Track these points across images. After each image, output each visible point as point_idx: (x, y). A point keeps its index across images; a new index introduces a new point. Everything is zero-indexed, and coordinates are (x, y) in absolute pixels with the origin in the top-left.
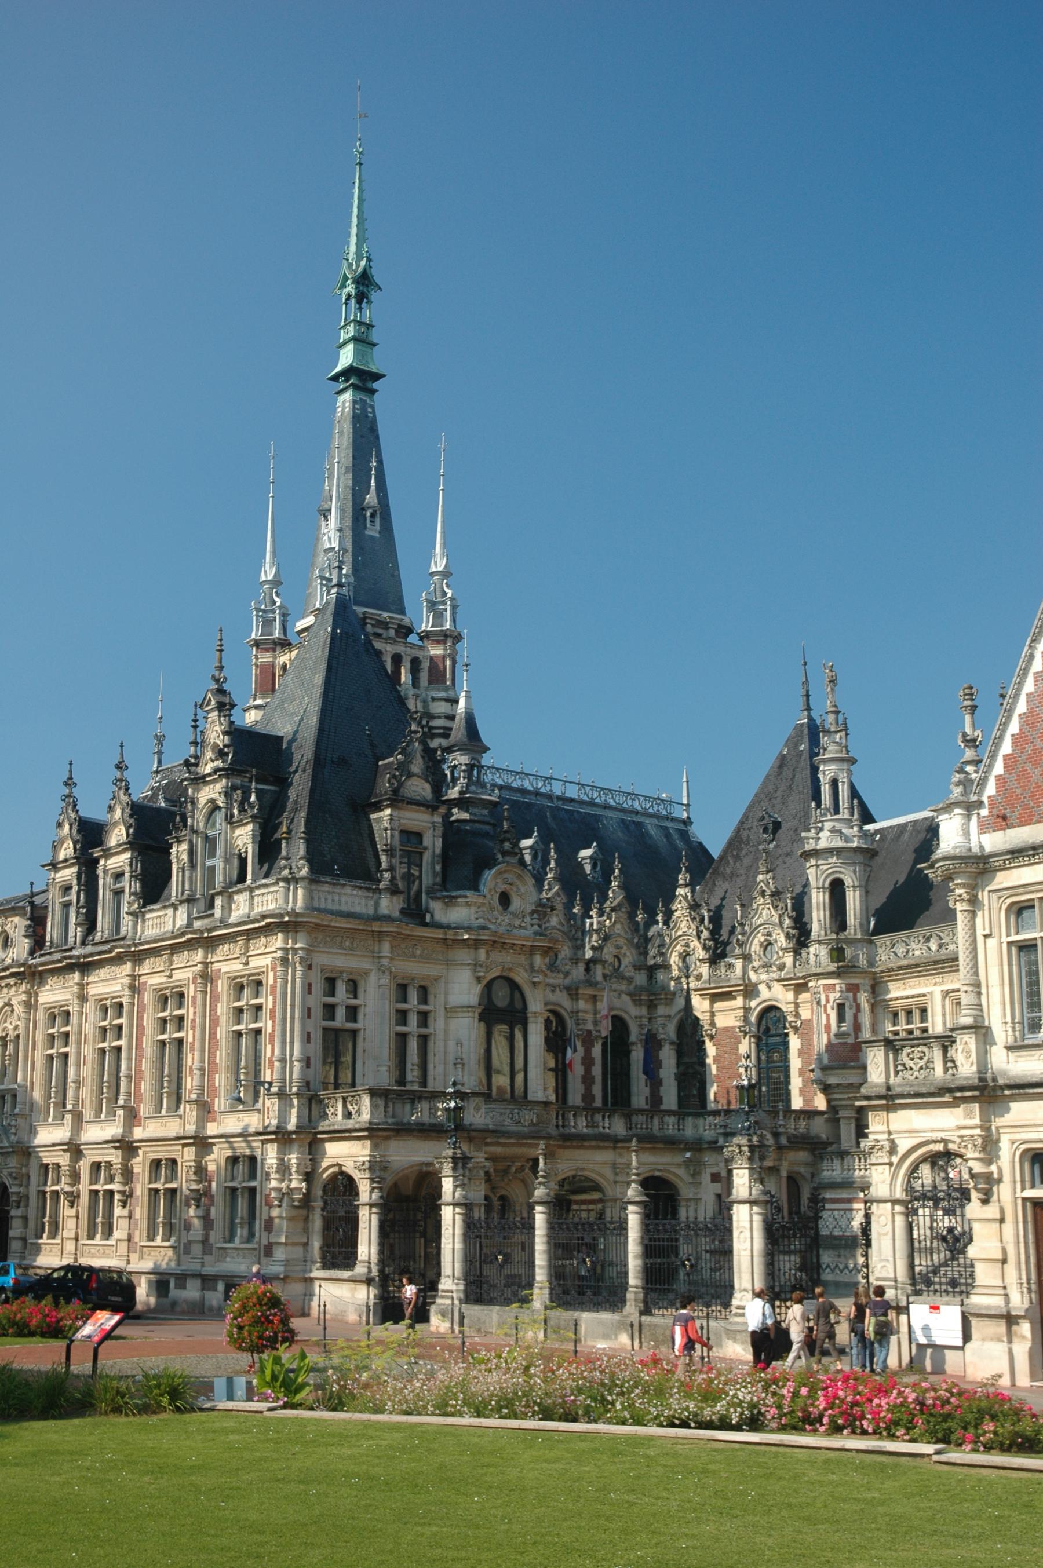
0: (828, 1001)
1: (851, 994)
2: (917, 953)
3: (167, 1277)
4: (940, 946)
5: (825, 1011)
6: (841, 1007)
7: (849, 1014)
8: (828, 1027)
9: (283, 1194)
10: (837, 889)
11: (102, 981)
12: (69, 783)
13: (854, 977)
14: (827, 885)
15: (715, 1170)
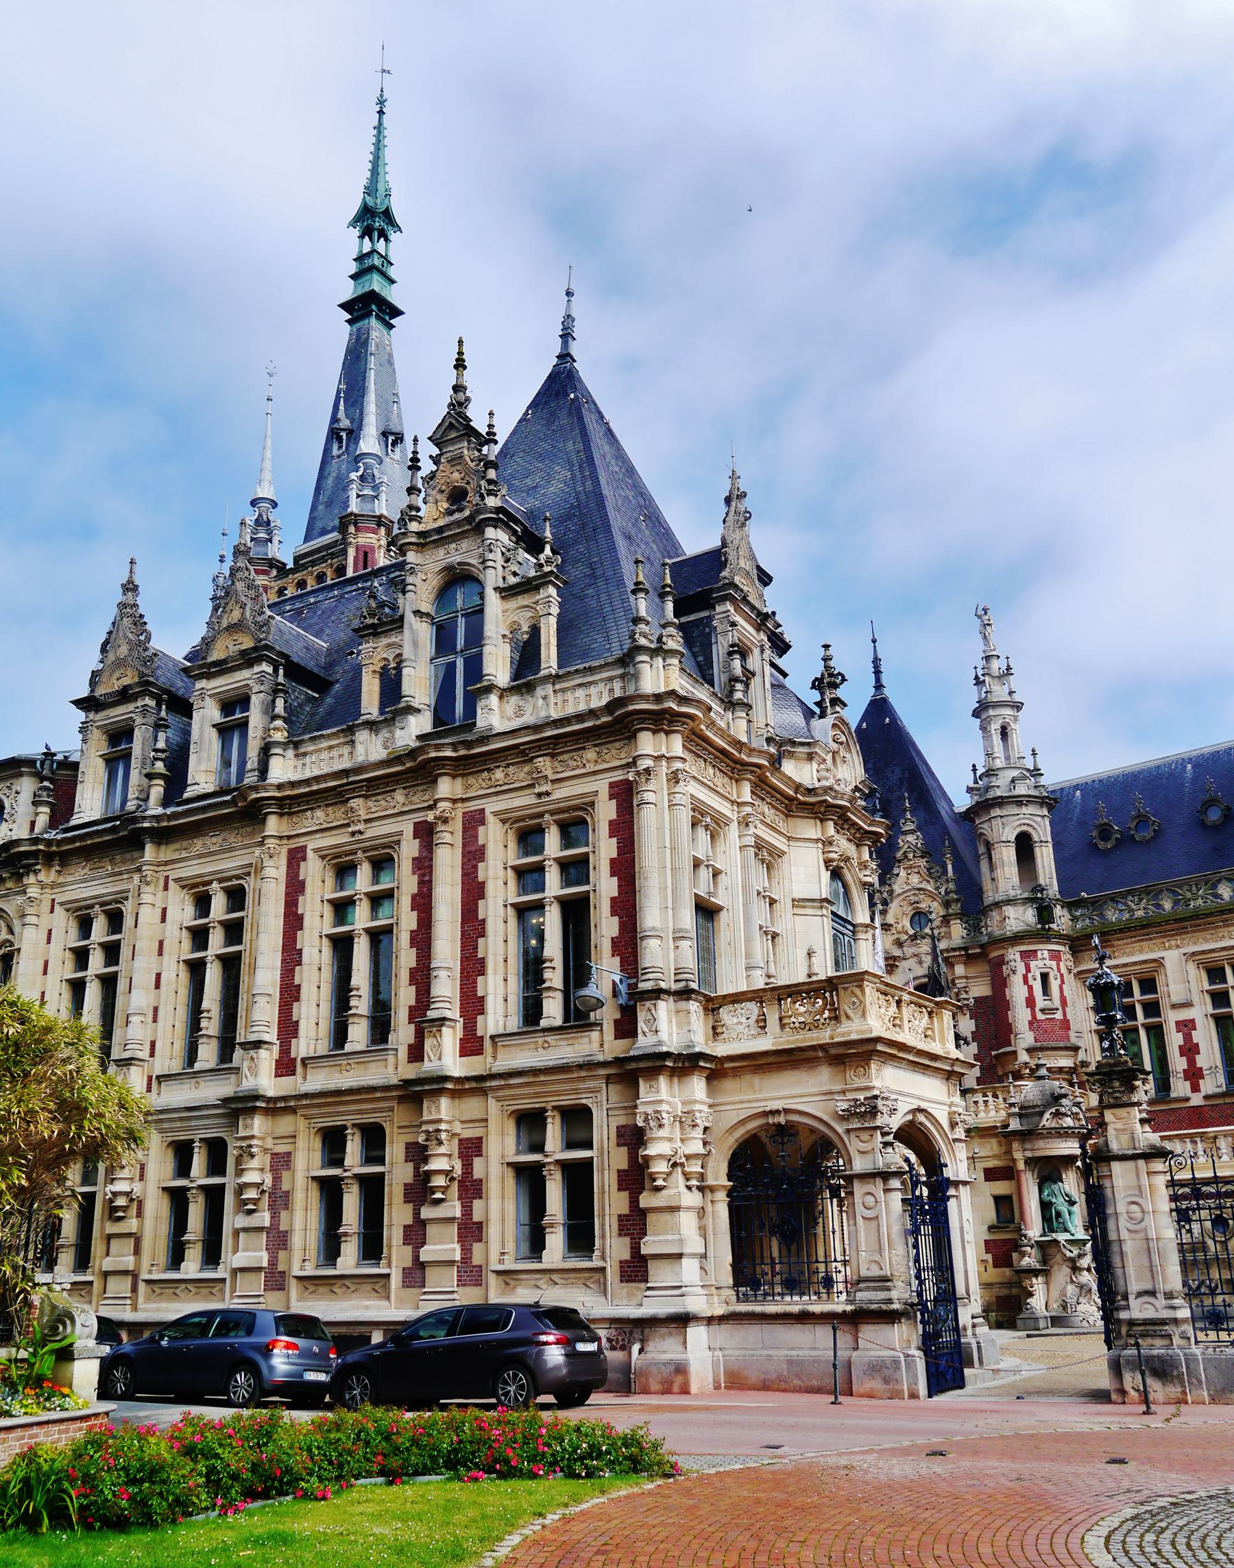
0: (1028, 970)
1: (1054, 964)
2: (1140, 913)
3: (363, 1329)
4: (1176, 903)
5: (1026, 981)
6: (1045, 977)
7: (1054, 985)
8: (1030, 1002)
9: (675, 1165)
10: (1024, 845)
11: (200, 856)
12: (130, 587)
13: (1057, 943)
14: (1013, 839)
15: (992, 1164)
